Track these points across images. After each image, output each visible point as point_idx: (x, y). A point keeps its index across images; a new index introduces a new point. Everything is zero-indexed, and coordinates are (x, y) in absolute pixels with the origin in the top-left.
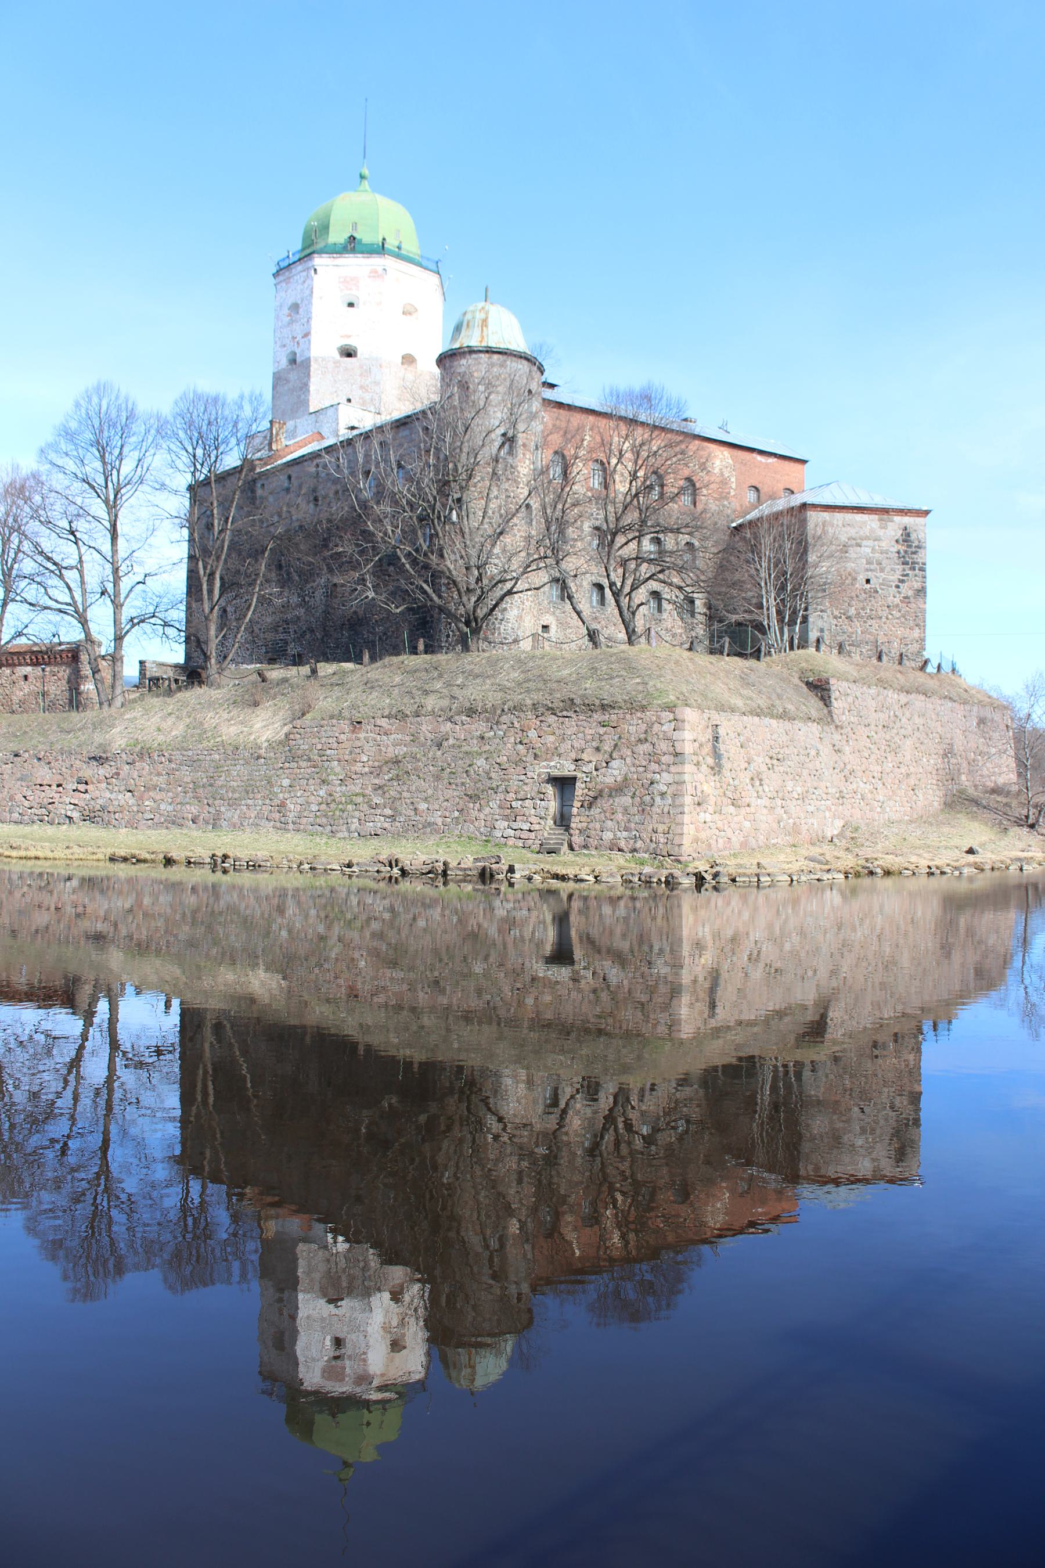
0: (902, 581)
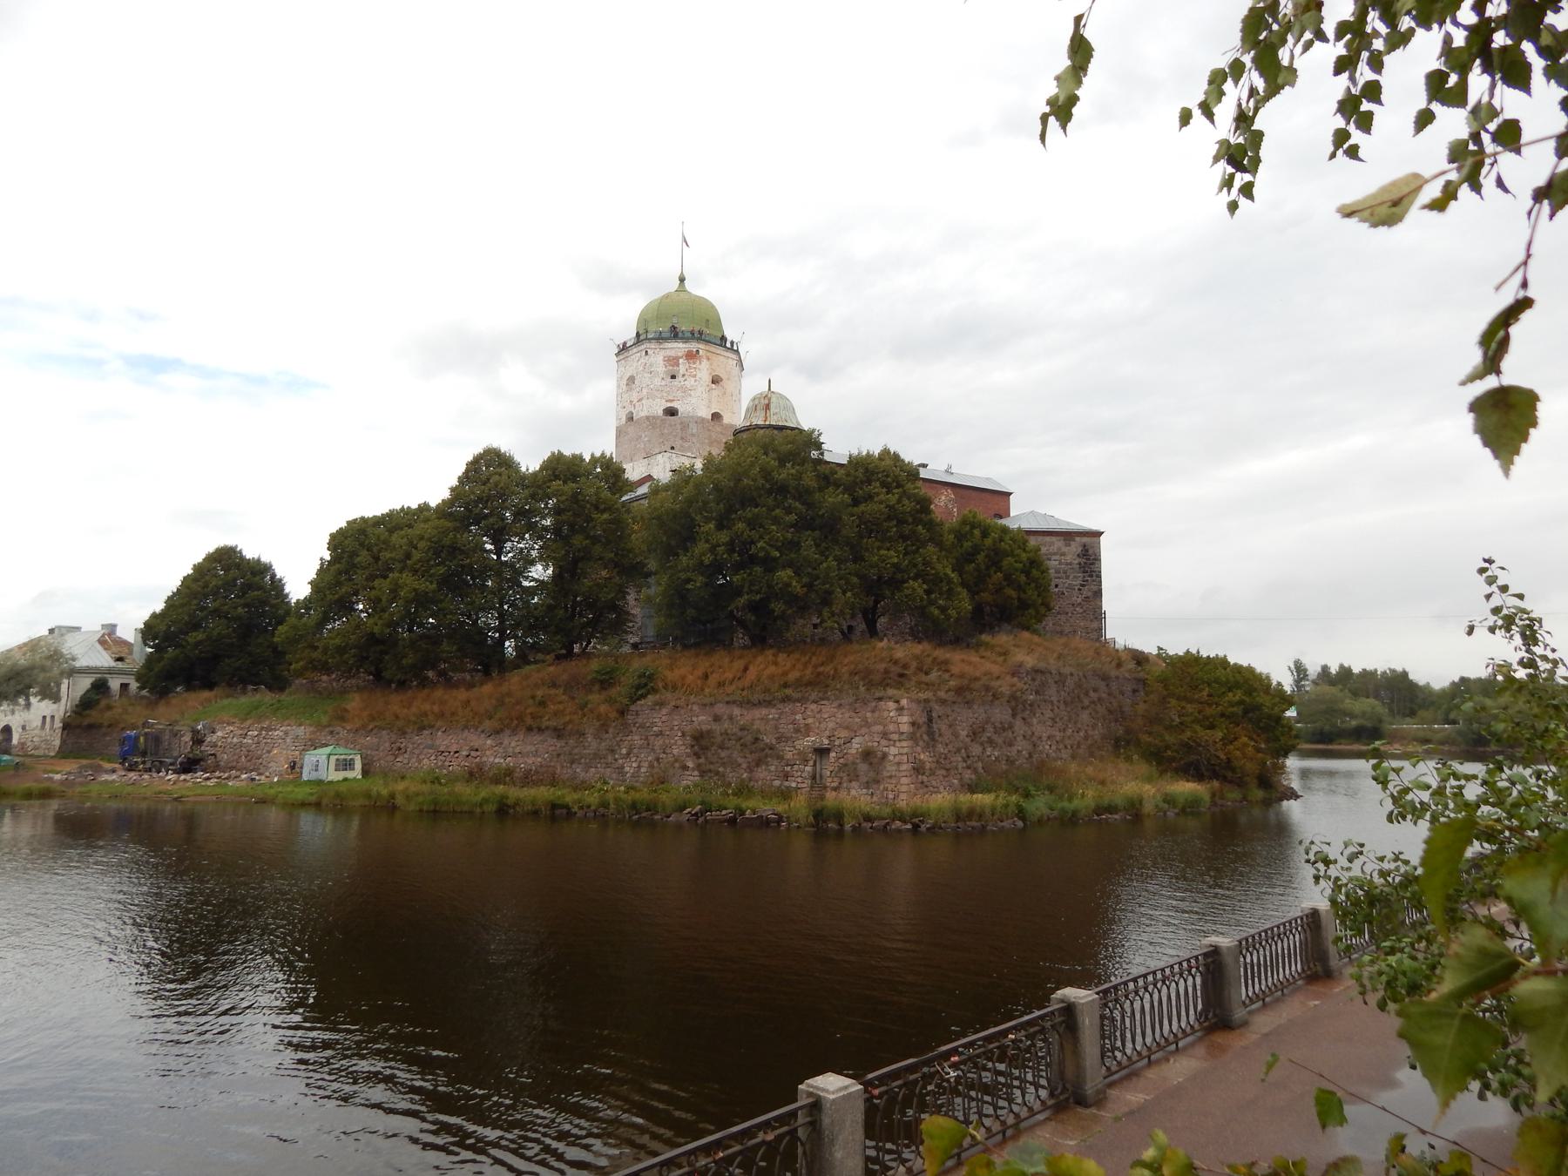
0: (1083, 585)
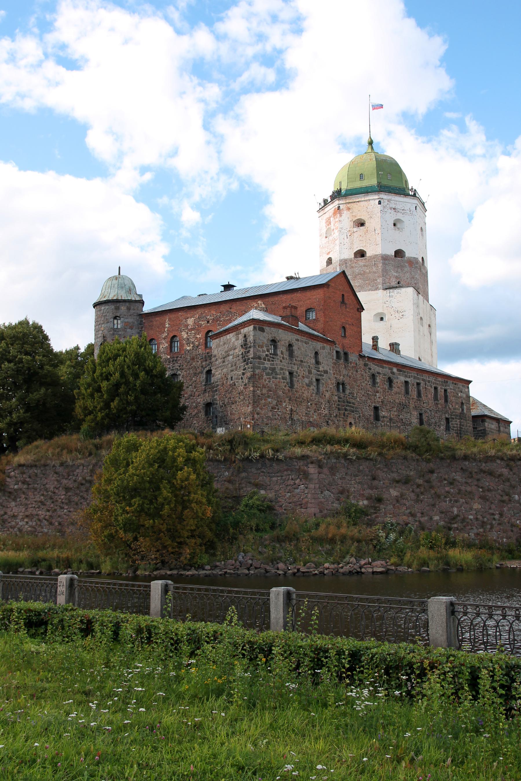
0: (243, 374)
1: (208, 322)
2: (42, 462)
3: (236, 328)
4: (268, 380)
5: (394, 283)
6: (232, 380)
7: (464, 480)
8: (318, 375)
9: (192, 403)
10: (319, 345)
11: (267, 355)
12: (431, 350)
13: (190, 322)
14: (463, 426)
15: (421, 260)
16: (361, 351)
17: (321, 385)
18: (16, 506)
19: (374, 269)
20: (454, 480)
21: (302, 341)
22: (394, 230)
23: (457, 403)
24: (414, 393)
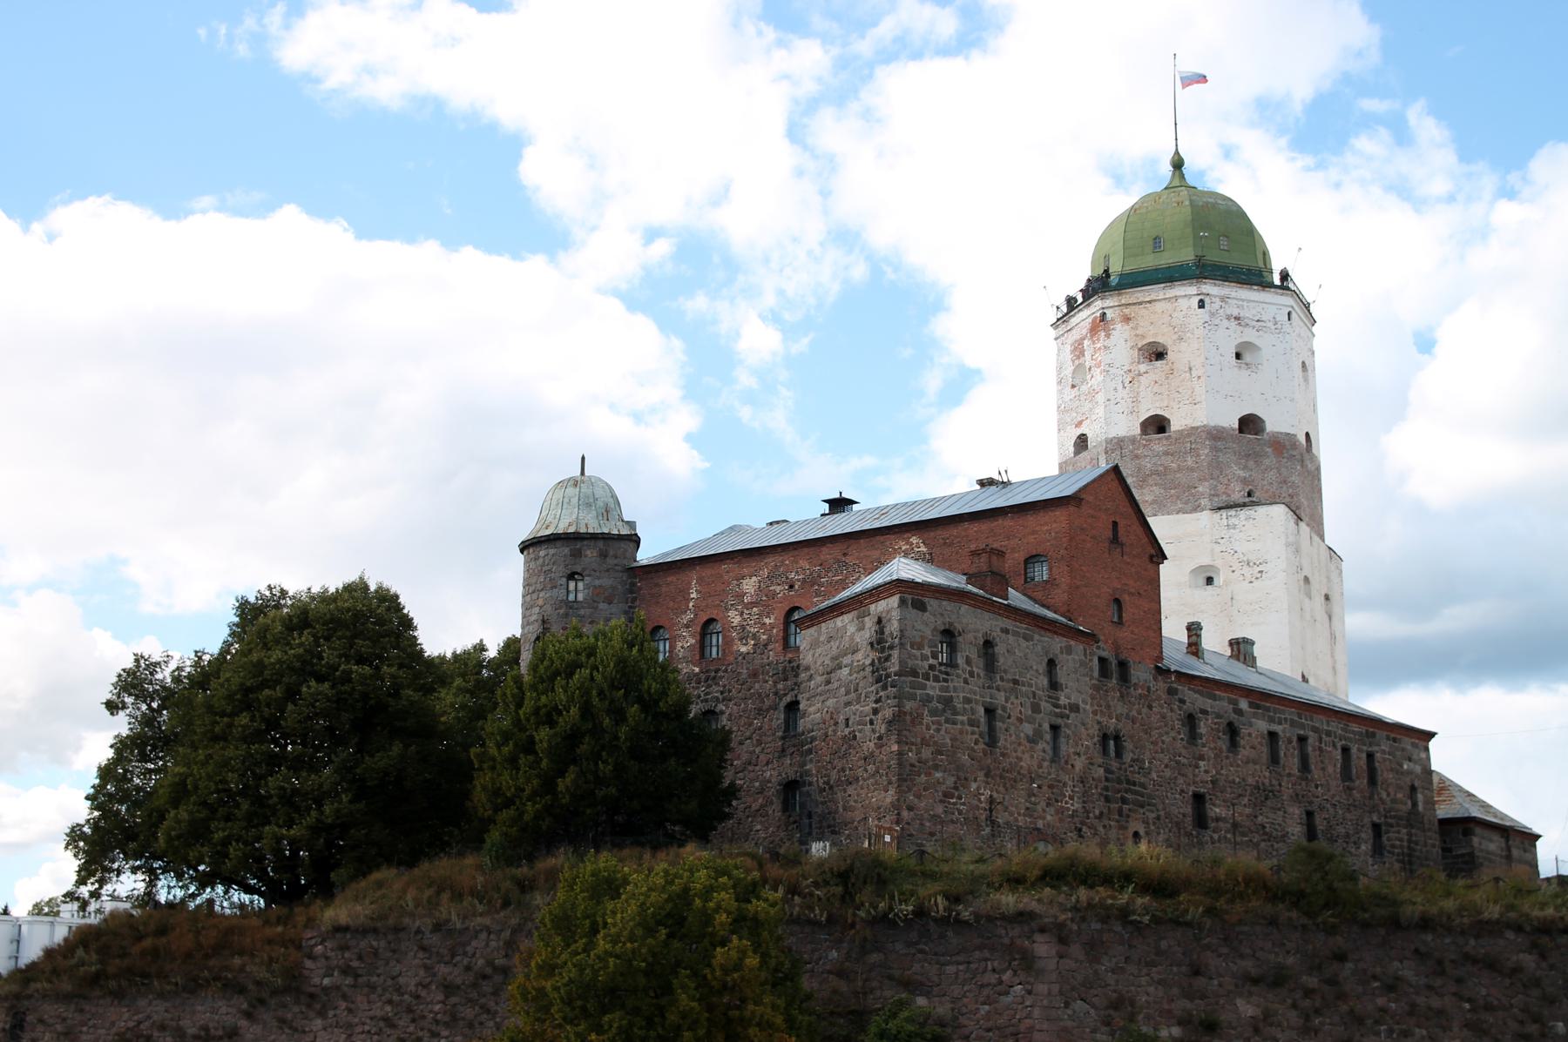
0: (875, 711)
1: (791, 587)
2: (391, 921)
3: (858, 603)
4: (934, 727)
5: (1238, 495)
6: (847, 726)
7: (1423, 981)
8: (1057, 715)
9: (752, 781)
10: (1057, 644)
11: (932, 667)
12: (1333, 656)
13: (749, 586)
14: (1417, 844)
15: (1303, 439)
16: (1160, 658)
17: (1063, 740)
18: (325, 1029)
19: (1190, 461)
20: (1397, 978)
21: (1016, 634)
22: (1236, 369)
23: (1400, 788)
24: (1291, 762)
